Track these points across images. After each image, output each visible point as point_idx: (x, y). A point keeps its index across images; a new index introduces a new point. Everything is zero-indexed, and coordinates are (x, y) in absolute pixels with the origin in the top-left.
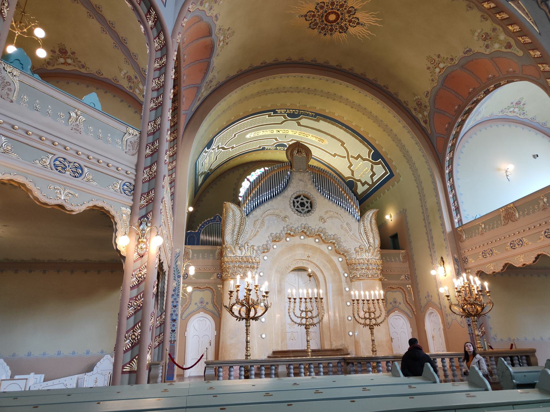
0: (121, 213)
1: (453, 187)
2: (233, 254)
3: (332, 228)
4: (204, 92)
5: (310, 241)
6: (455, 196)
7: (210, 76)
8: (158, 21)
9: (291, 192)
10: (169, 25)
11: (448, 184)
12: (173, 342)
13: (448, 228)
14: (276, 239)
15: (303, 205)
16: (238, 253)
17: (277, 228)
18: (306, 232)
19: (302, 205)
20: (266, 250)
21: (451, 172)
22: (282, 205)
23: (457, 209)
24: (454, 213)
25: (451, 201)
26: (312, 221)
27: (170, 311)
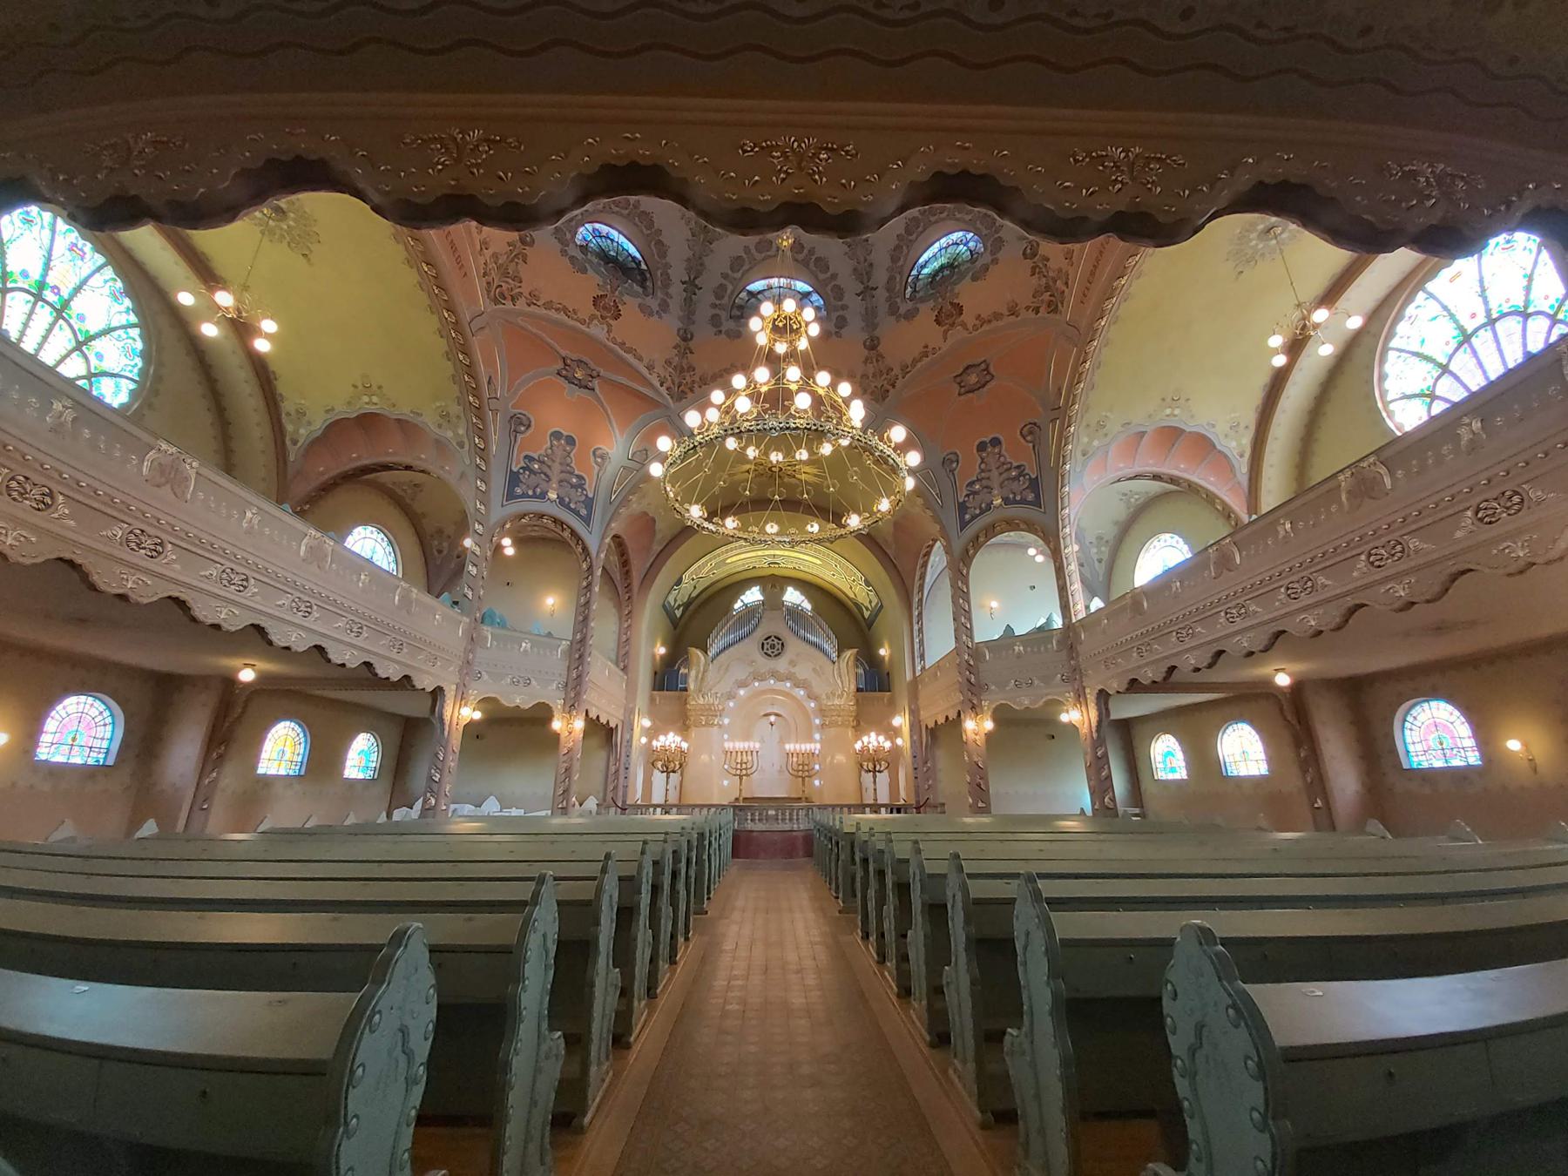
0: (557, 704)
1: (920, 630)
2: (696, 701)
3: (803, 672)
4: (657, 548)
5: (780, 686)
6: (921, 642)
7: (659, 536)
8: (585, 549)
9: (760, 634)
10: (593, 549)
11: (916, 627)
12: (626, 787)
13: (909, 677)
14: (743, 685)
15: (773, 646)
16: (701, 701)
17: (741, 673)
18: (775, 675)
19: (773, 647)
20: (731, 696)
21: (920, 614)
22: (751, 647)
23: (922, 657)
24: (917, 660)
25: (916, 646)
26: (781, 664)
27: (623, 758)
